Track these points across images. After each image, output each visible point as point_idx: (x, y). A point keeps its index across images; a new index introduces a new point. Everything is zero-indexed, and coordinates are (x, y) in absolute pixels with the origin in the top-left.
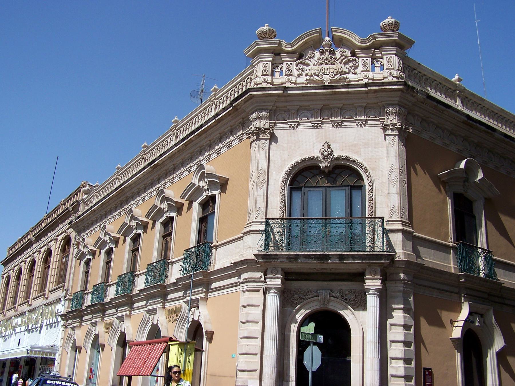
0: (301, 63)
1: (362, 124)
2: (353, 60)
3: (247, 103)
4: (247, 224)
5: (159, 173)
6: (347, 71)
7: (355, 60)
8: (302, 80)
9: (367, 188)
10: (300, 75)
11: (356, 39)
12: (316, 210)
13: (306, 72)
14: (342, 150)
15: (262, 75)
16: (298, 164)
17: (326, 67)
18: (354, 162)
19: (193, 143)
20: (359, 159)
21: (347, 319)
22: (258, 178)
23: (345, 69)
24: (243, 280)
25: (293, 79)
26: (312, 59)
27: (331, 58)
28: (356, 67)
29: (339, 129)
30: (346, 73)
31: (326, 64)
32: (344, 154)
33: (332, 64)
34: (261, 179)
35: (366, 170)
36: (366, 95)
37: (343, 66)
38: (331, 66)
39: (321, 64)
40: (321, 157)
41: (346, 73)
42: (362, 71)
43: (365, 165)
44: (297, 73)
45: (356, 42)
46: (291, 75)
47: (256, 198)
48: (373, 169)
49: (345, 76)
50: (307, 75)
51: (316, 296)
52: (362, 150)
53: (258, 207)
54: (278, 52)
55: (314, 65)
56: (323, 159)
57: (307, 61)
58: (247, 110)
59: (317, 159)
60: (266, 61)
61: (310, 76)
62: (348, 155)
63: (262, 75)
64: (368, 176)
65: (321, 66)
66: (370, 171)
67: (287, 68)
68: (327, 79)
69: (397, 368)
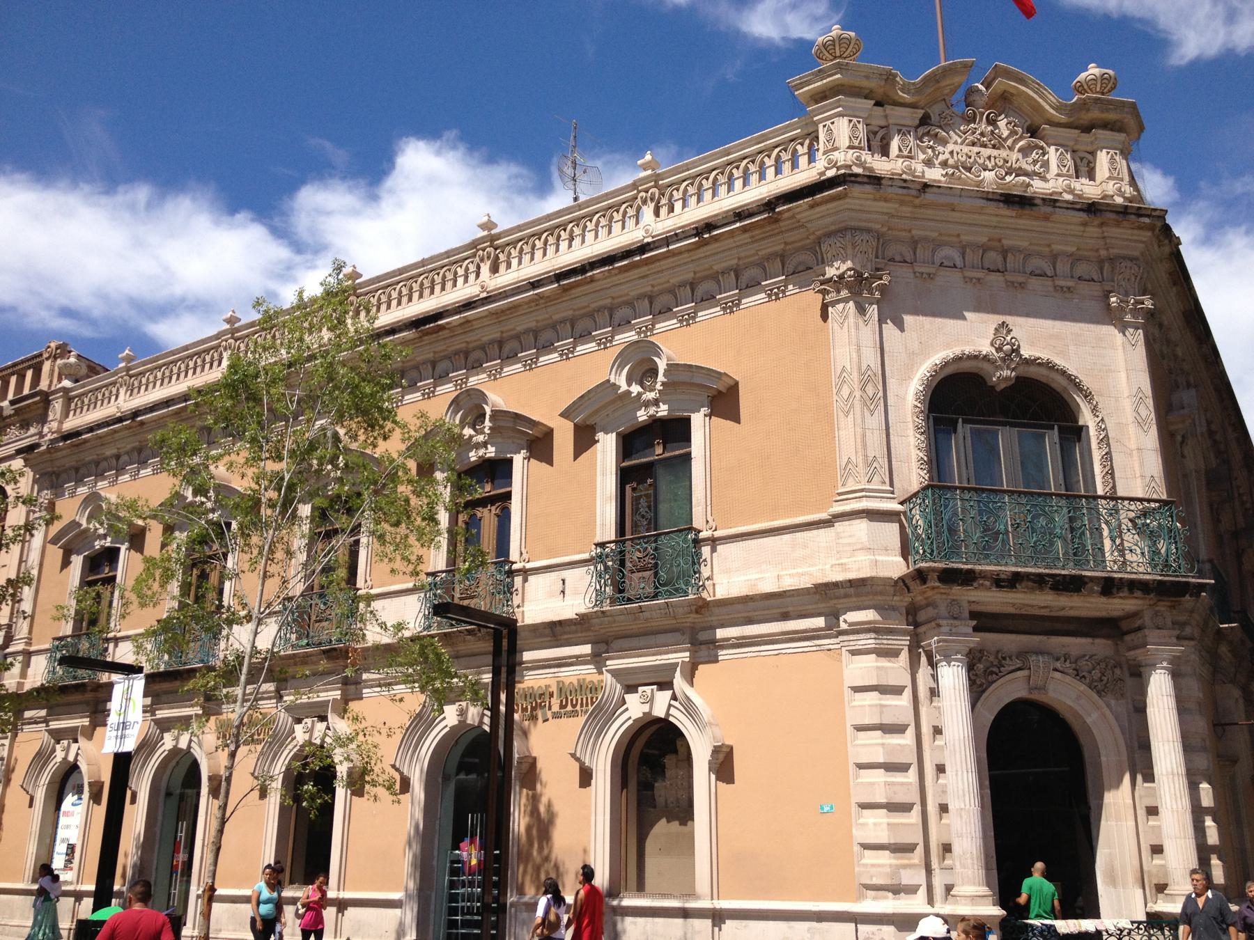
2: (1037, 147)
3: (818, 209)
4: (840, 494)
5: (440, 347)
7: (1042, 148)
9: (1093, 432)
10: (929, 163)
11: (1048, 102)
13: (941, 158)
14: (1032, 344)
15: (850, 147)
16: (946, 364)
17: (986, 152)
18: (1063, 373)
19: (594, 285)
20: (1072, 371)
22: (863, 389)
24: (851, 624)
27: (992, 132)
31: (985, 146)
33: (994, 147)
34: (870, 390)
35: (1088, 396)
36: (1082, 228)
38: (995, 152)
39: (973, 144)
42: (1058, 175)
43: (1087, 383)
45: (1047, 107)
46: (911, 158)
47: (864, 436)
50: (944, 164)
51: (1019, 669)
52: (1072, 348)
53: (871, 455)
54: (879, 98)
55: (956, 143)
56: (1003, 359)
59: (986, 358)
61: (952, 167)
62: (1052, 358)
63: (850, 147)
64: (1095, 410)
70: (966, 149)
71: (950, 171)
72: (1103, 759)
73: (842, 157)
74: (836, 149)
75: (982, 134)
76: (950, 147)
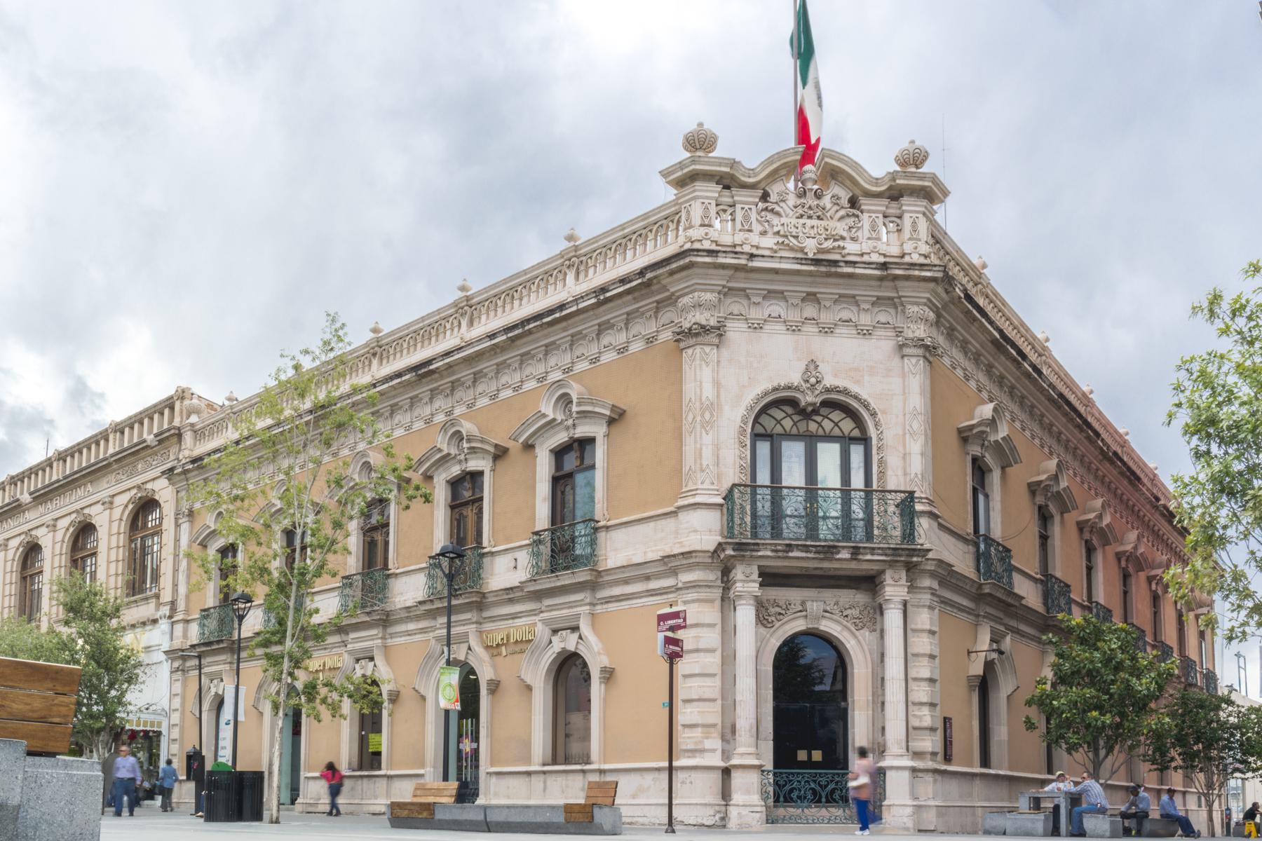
0: (766, 209)
1: (865, 333)
6: (845, 234)
8: (769, 242)
9: (874, 442)
10: (764, 233)
12: (793, 475)
13: (776, 229)
14: (836, 376)
15: (702, 225)
17: (809, 222)
18: (856, 397)
21: (848, 646)
23: (840, 228)
25: (755, 238)
26: (782, 204)
27: (818, 206)
28: (859, 228)
29: (830, 340)
30: (843, 238)
31: (810, 217)
32: (841, 383)
33: (819, 218)
35: (874, 415)
37: (838, 225)
39: (802, 216)
40: (805, 386)
41: (843, 238)
43: (873, 405)
44: (760, 228)
45: (862, 182)
46: (750, 231)
48: (884, 412)
49: (841, 243)
50: (778, 233)
52: (866, 378)
54: (727, 182)
57: (777, 208)
58: (672, 290)
60: (707, 198)
64: (877, 425)
65: (802, 221)
66: (880, 416)
67: (744, 216)
68: (811, 246)
69: (920, 717)
70: (794, 221)
71: (781, 240)
72: (856, 671)
73: (697, 233)
74: (691, 227)
75: (810, 208)
76: (784, 220)
